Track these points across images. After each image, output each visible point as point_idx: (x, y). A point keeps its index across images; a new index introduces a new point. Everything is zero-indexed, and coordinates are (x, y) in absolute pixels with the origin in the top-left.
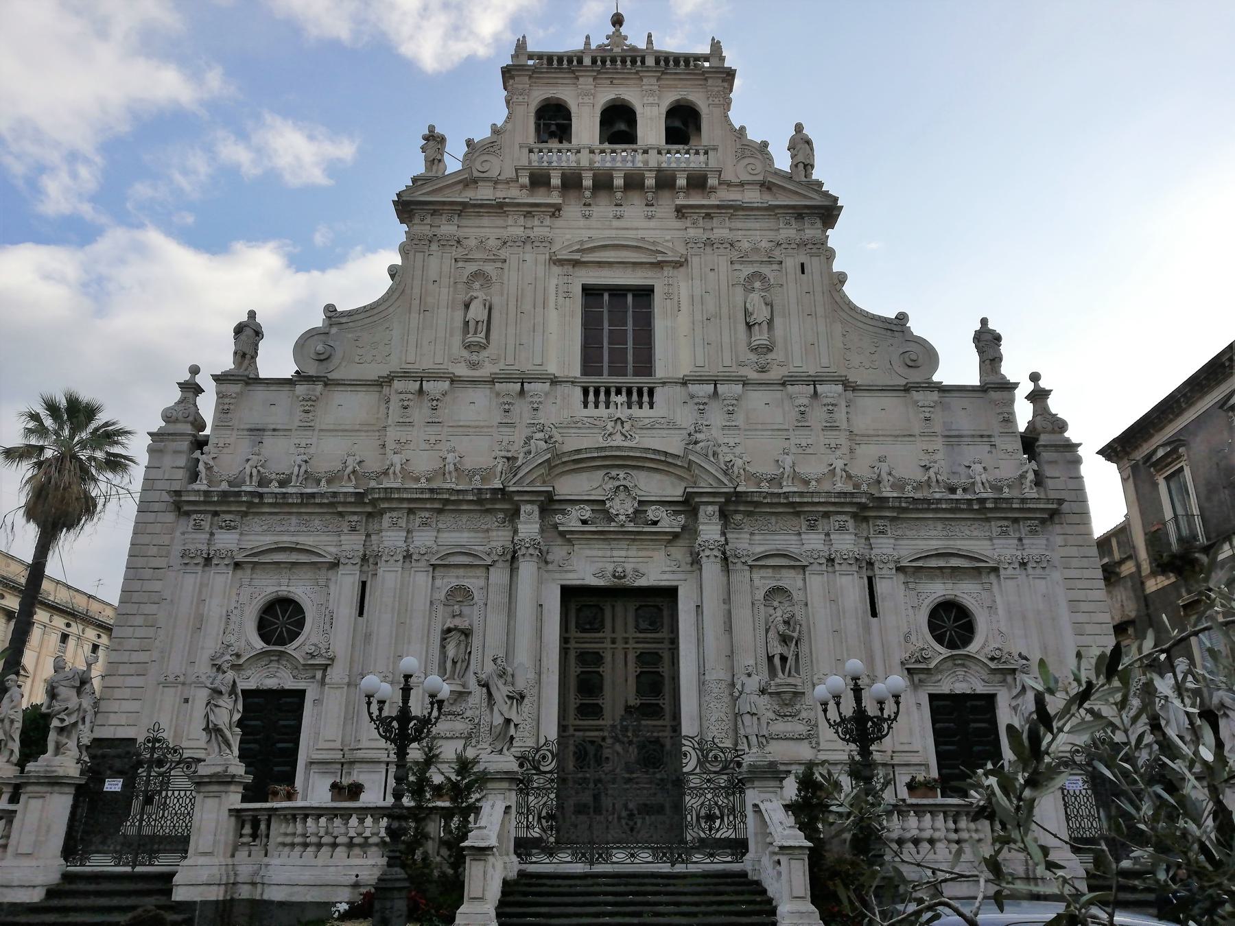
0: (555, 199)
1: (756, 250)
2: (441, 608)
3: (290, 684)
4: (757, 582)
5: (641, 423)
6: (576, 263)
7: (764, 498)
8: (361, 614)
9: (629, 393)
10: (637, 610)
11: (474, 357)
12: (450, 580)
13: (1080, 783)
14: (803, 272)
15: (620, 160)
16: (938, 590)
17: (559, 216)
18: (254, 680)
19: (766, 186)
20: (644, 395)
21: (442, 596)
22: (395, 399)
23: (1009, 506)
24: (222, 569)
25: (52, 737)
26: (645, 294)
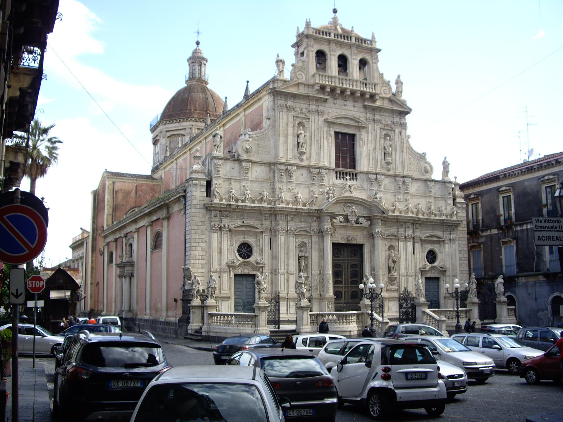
1: (387, 125)
12: (299, 240)
26: (353, 136)
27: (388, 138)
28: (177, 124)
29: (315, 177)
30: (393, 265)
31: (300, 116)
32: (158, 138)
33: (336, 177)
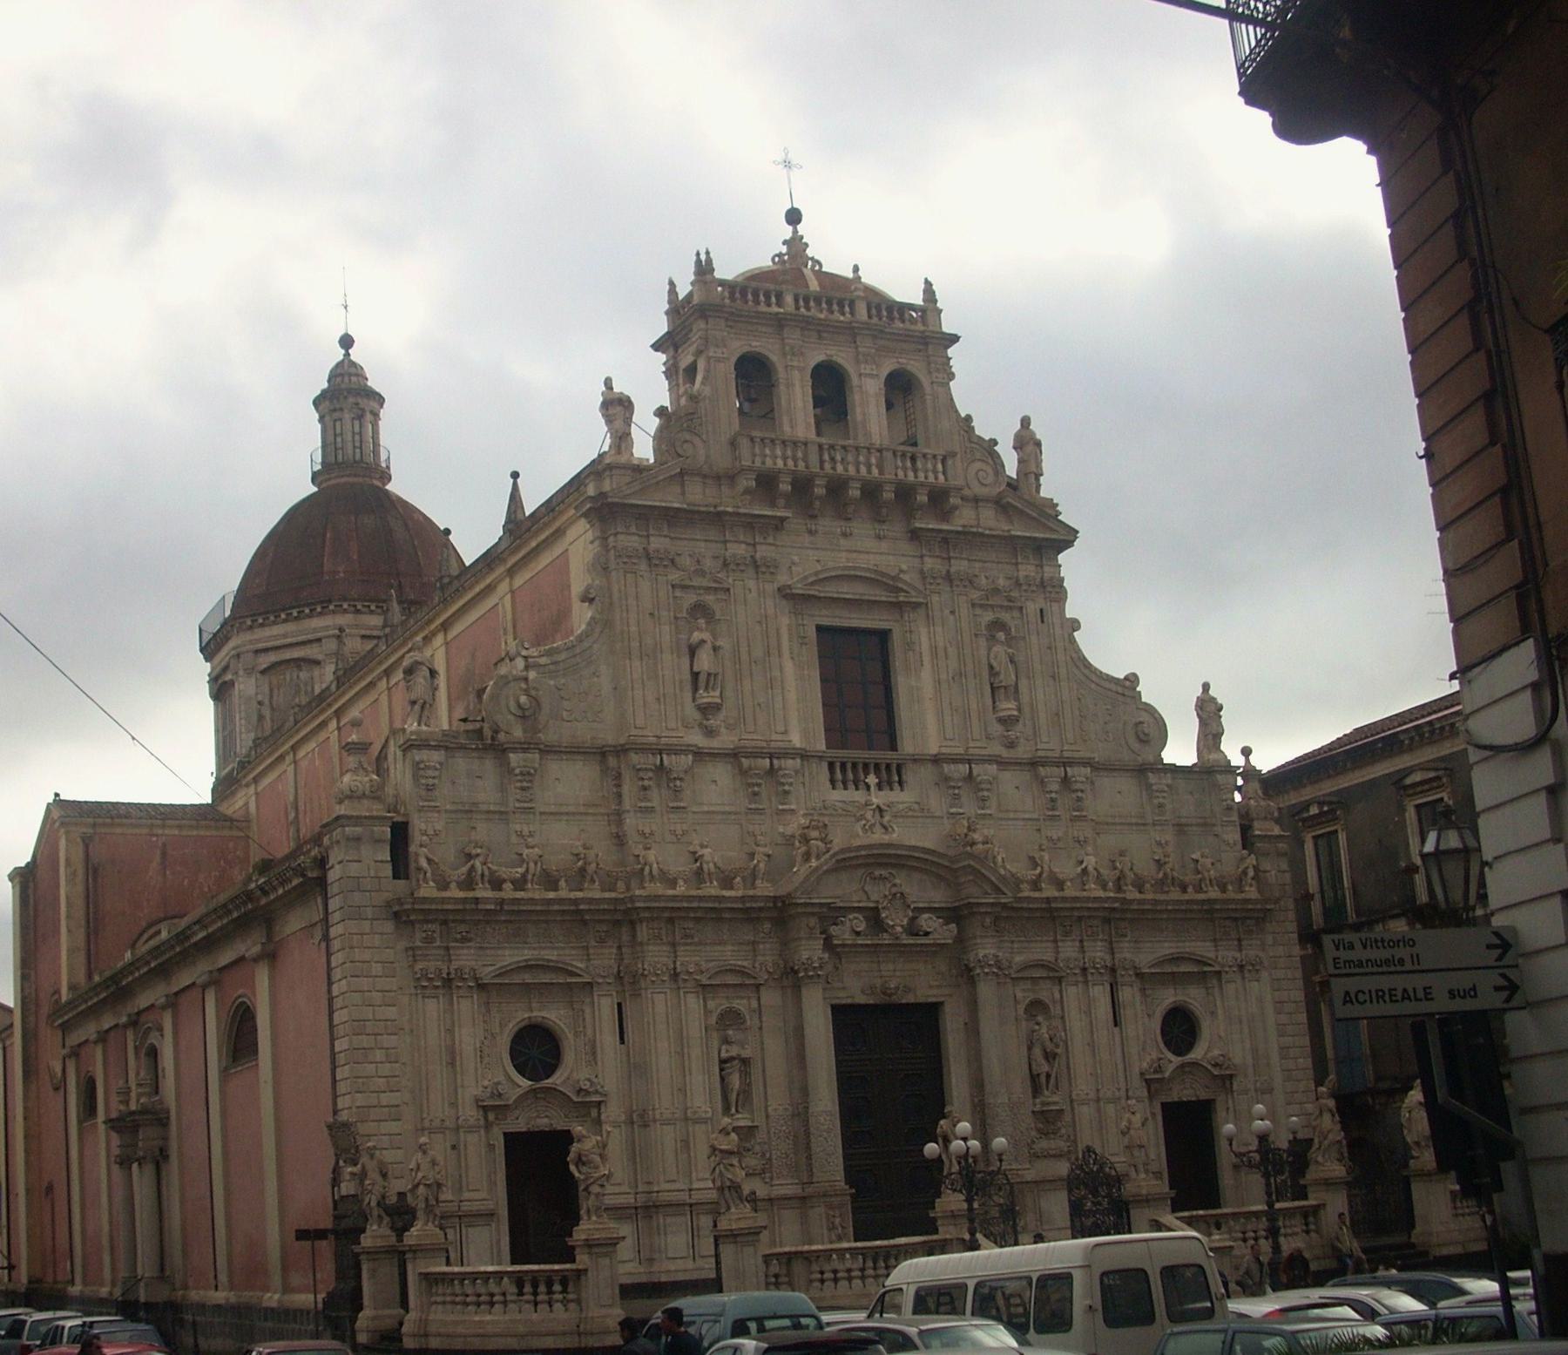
1: (996, 591)
3: (560, 1125)
8: (622, 1041)
12: (718, 1004)
18: (520, 1123)
21: (713, 1020)
22: (627, 776)
27: (1001, 636)
28: (290, 627)
29: (759, 785)
30: (1045, 1068)
31: (697, 582)
32: (228, 677)
33: (833, 782)
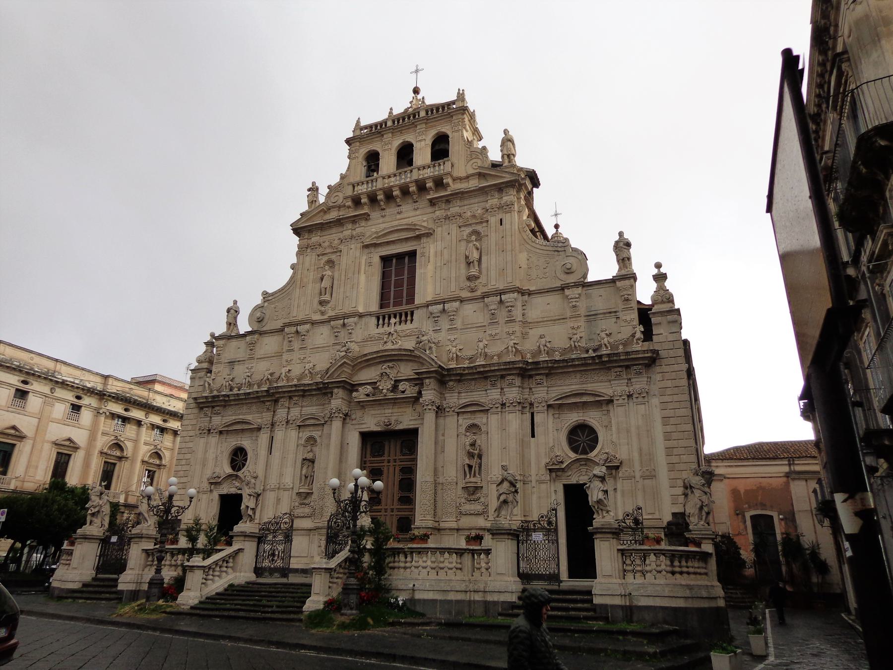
0: (366, 210)
1: (474, 216)
2: (302, 448)
4: (460, 421)
5: (404, 333)
6: (375, 245)
7: (464, 370)
9: (401, 317)
10: (402, 443)
11: (473, 285)
12: (306, 434)
13: (541, 536)
14: (501, 224)
15: (410, 177)
16: (574, 418)
17: (370, 219)
19: (481, 176)
20: (407, 316)
21: (302, 442)
23: (618, 358)
24: (214, 435)
25: (89, 518)
26: (412, 254)
